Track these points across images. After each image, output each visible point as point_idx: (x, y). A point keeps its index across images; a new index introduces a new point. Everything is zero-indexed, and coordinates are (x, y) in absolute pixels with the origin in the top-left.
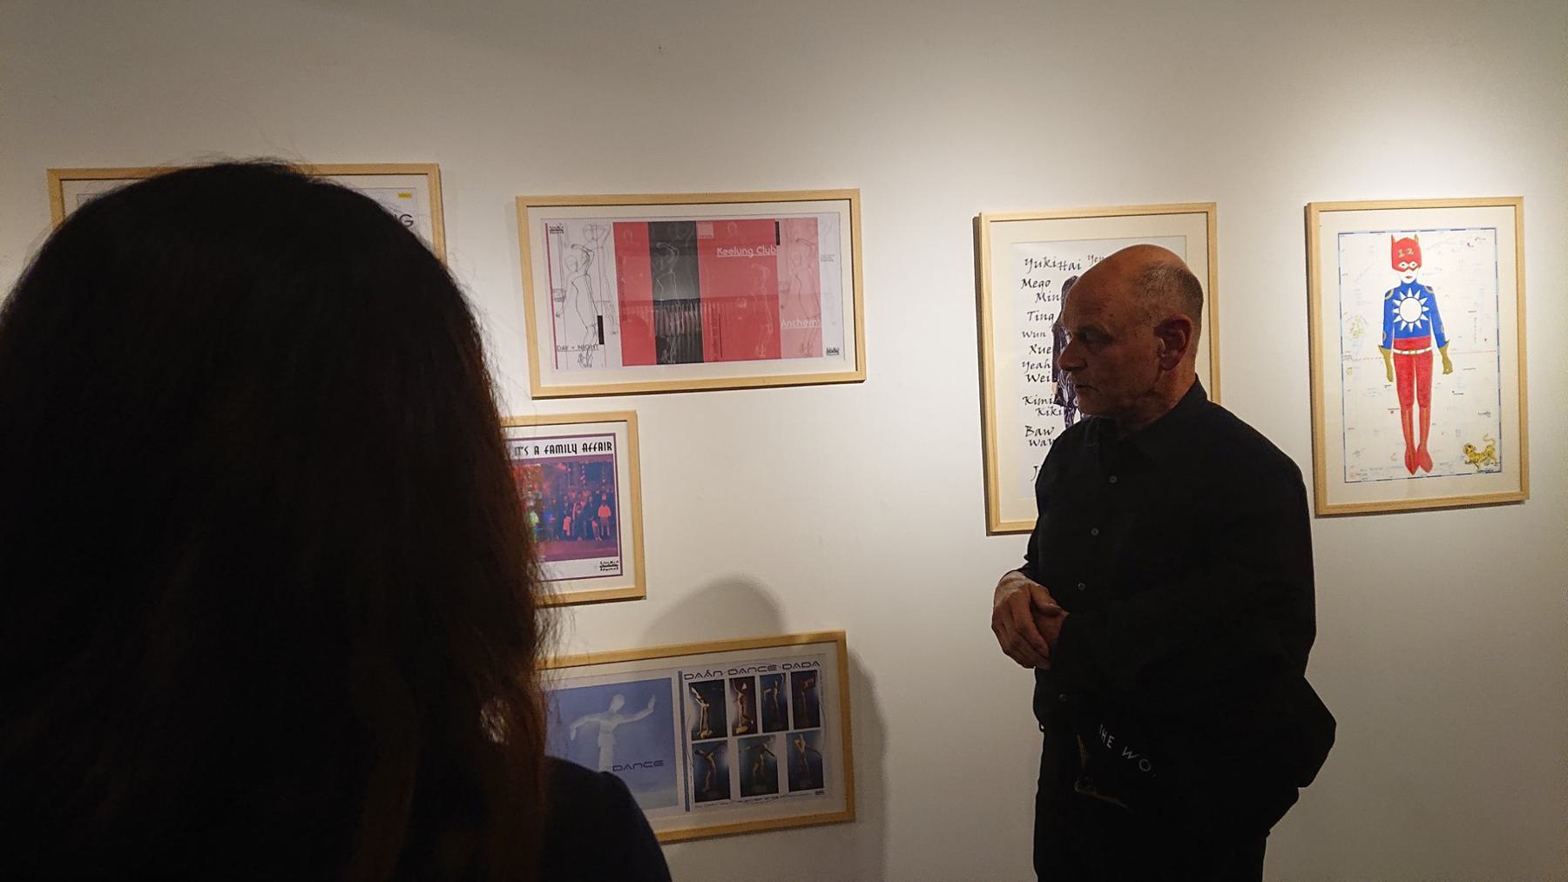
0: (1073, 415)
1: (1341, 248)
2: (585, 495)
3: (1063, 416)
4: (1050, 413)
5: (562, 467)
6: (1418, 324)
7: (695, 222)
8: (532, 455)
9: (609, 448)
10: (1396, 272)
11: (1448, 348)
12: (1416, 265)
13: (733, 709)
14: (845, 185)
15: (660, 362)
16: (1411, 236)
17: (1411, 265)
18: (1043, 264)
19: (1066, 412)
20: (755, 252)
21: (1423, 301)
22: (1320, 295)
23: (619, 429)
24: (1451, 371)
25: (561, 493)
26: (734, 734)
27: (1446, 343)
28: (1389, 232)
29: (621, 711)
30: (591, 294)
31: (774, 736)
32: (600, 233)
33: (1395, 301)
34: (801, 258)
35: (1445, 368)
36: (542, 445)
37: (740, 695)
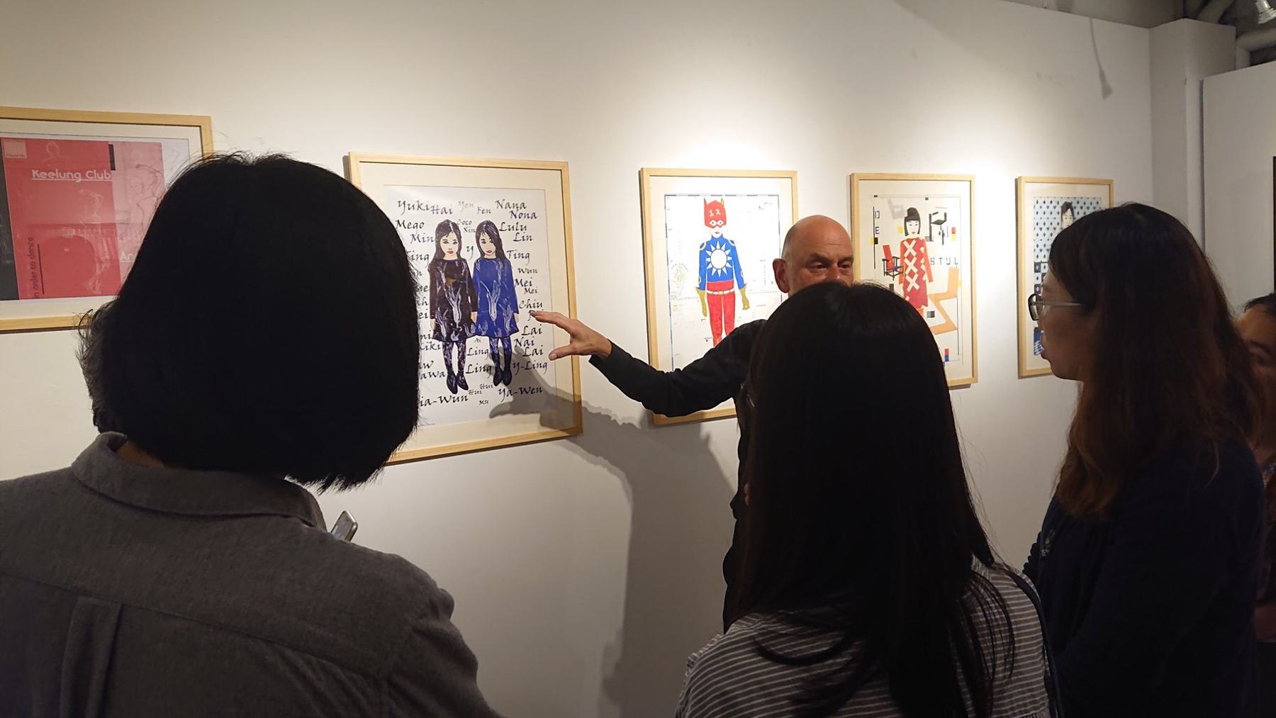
0: (451, 349)
1: (667, 208)
3: (441, 350)
4: (429, 347)
6: (725, 270)
10: (707, 228)
11: (746, 289)
12: (722, 223)
14: (198, 112)
16: (718, 199)
17: (718, 223)
18: (416, 207)
19: (444, 346)
20: (84, 176)
21: (728, 252)
22: (652, 245)
24: (748, 308)
27: (745, 285)
28: (702, 195)
33: (707, 252)
34: (143, 185)
35: (744, 305)
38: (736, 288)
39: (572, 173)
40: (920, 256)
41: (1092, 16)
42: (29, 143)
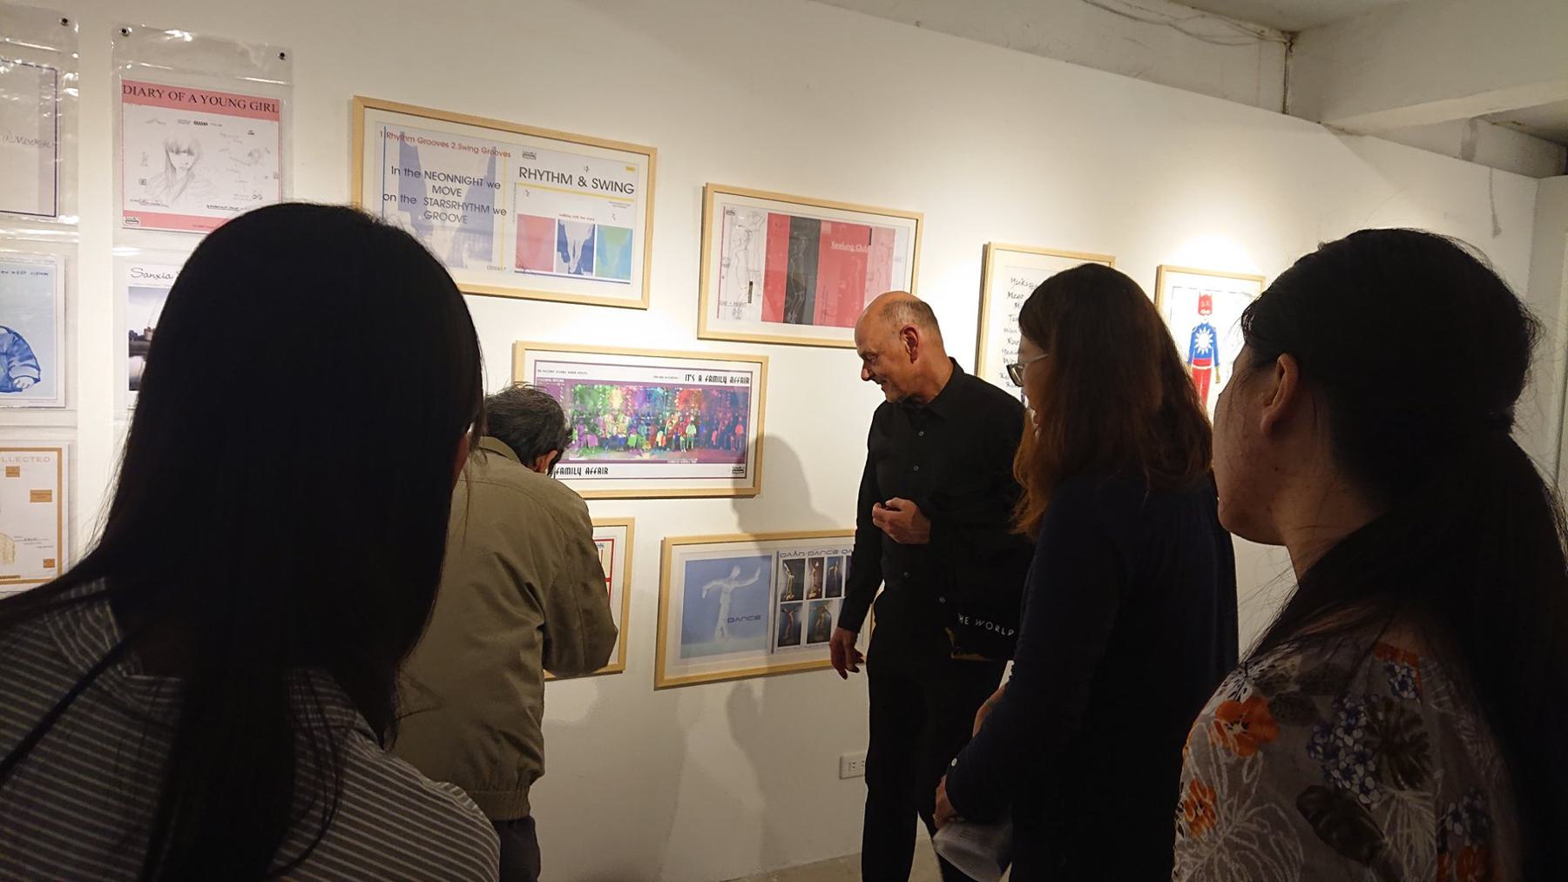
2: (728, 415)
5: (715, 393)
7: (819, 221)
8: (697, 382)
9: (748, 382)
13: (809, 580)
15: (785, 322)
16: (1209, 294)
23: (756, 368)
25: (712, 413)
26: (808, 598)
29: (736, 579)
30: (747, 263)
31: (832, 601)
32: (759, 218)
36: (705, 375)
37: (814, 570)
38: (1212, 366)
42: (834, 223)
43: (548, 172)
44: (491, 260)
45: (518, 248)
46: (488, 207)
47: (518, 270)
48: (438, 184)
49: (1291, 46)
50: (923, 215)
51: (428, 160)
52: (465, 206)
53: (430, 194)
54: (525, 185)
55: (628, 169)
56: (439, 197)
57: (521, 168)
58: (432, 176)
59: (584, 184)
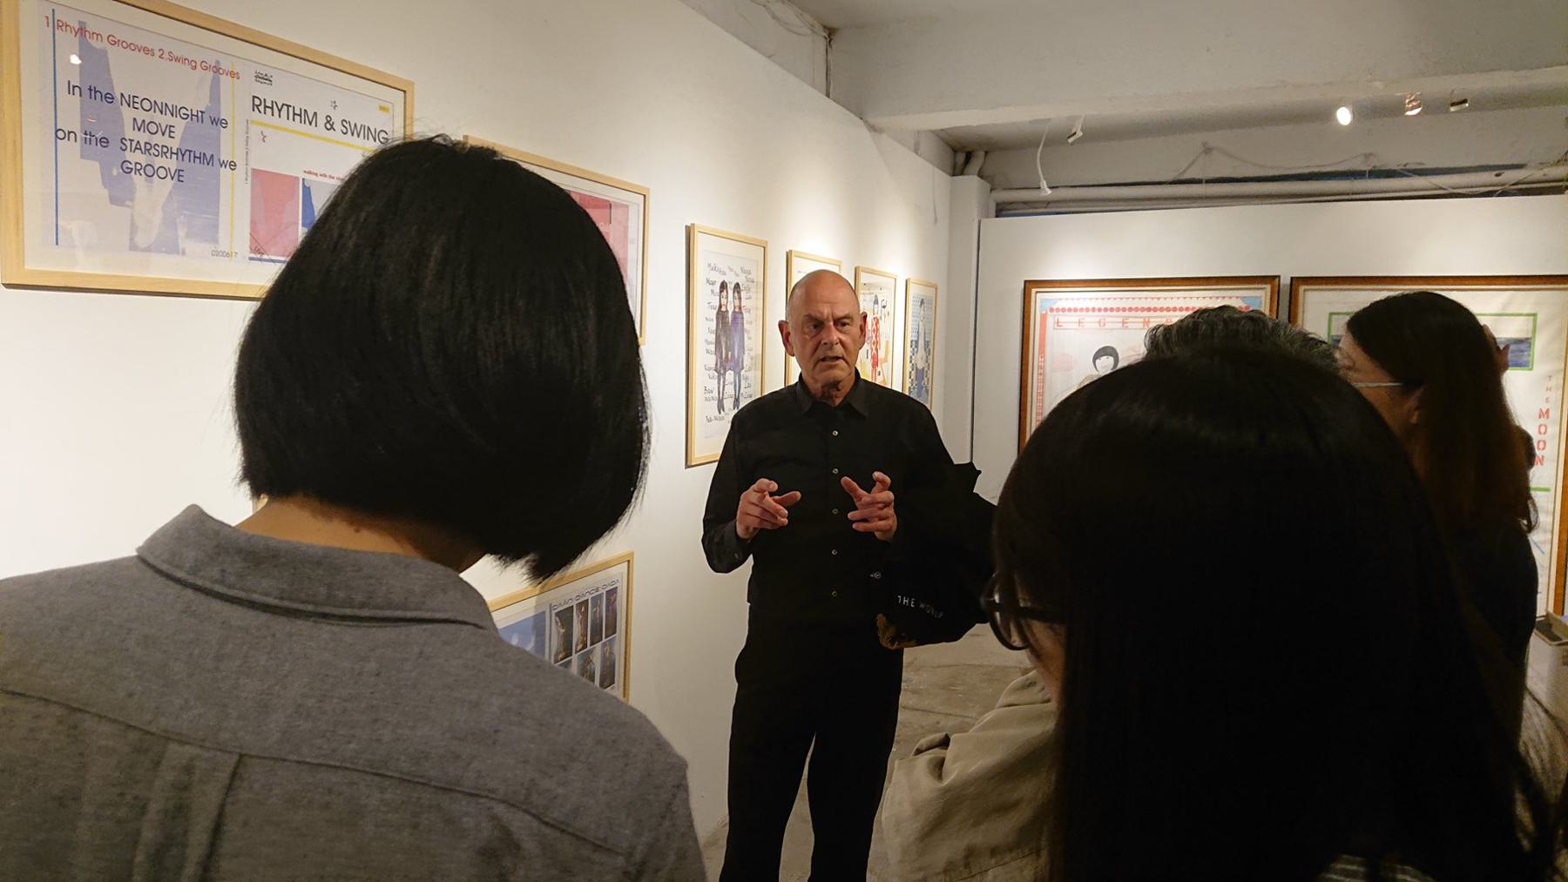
39: (768, 250)
40: (878, 330)
41: (933, 164)
43: (288, 106)
44: (216, 241)
45: (253, 223)
46: (212, 156)
47: (253, 255)
48: (141, 116)
49: (830, 42)
50: (648, 189)
51: (126, 76)
52: (181, 154)
53: (130, 133)
54: (261, 124)
55: (382, 108)
56: (143, 137)
57: (254, 97)
58: (132, 102)
59: (332, 126)
